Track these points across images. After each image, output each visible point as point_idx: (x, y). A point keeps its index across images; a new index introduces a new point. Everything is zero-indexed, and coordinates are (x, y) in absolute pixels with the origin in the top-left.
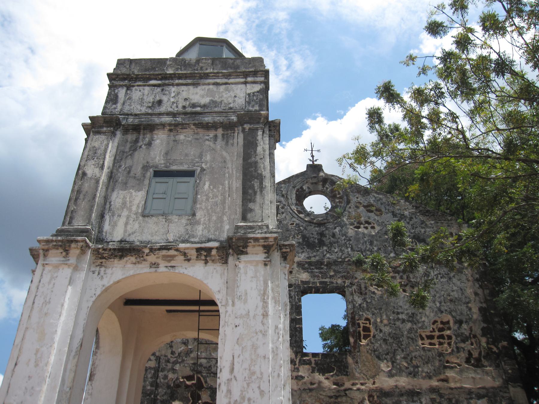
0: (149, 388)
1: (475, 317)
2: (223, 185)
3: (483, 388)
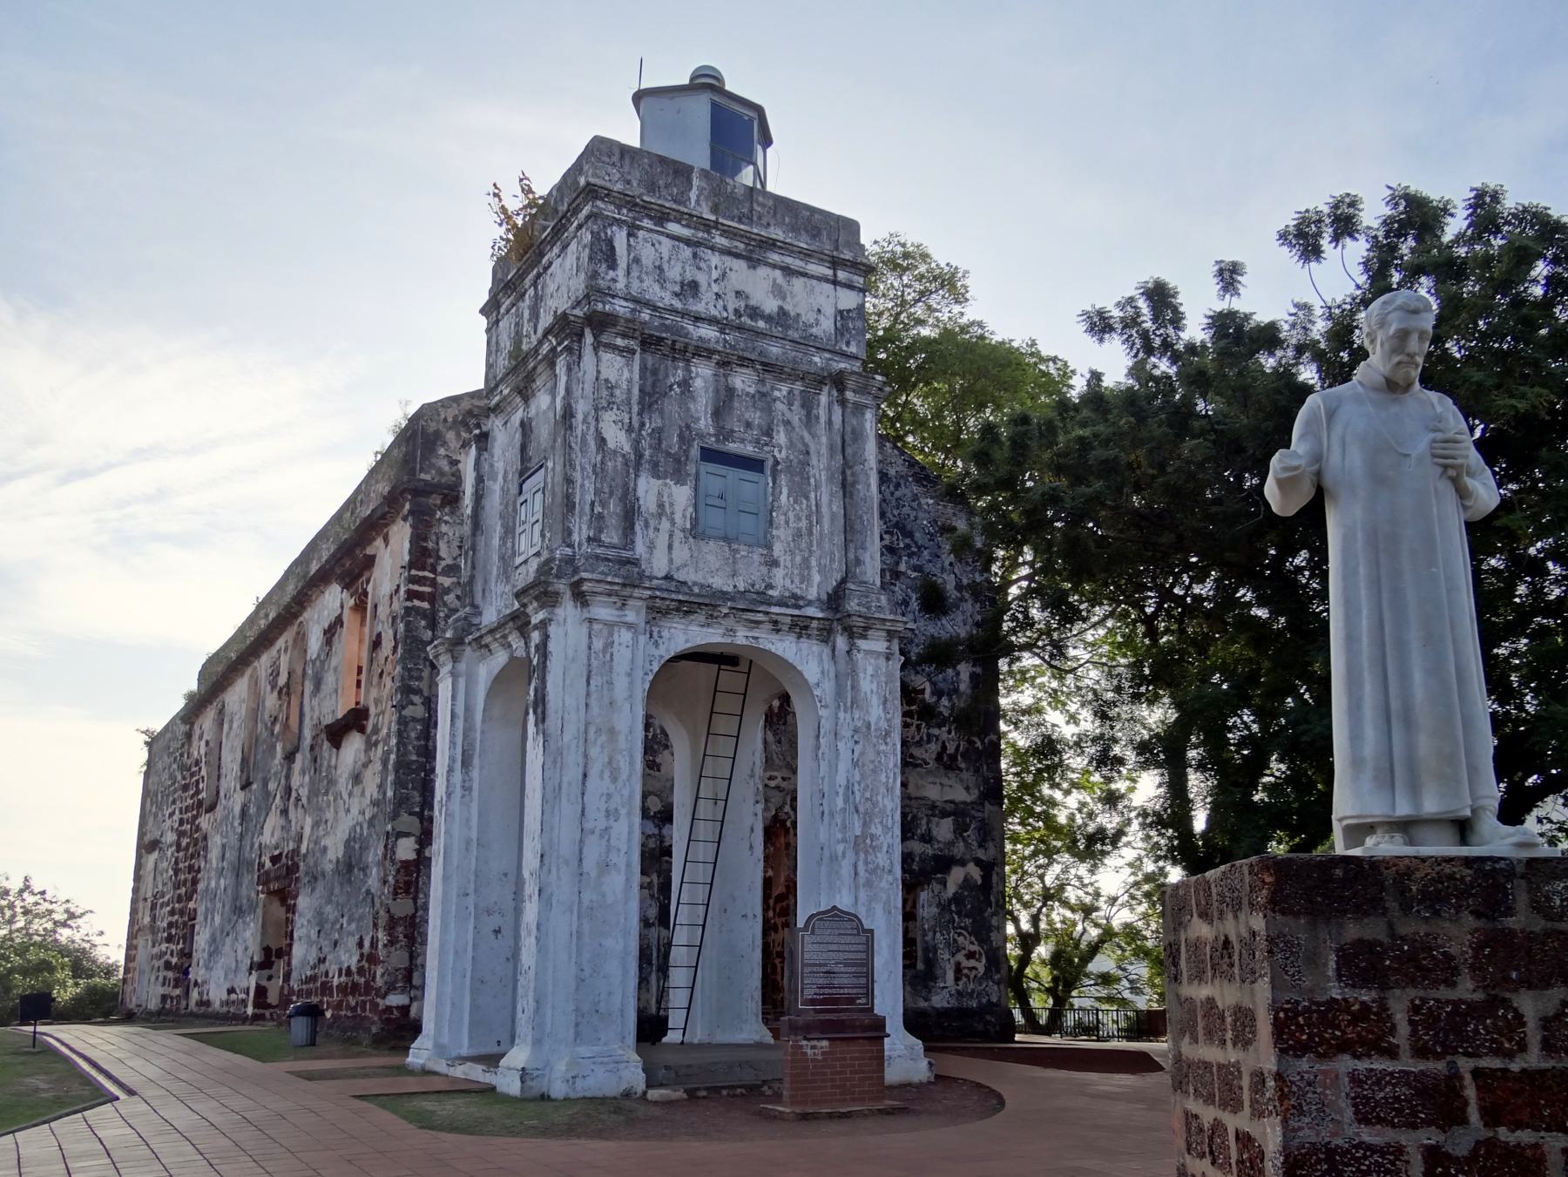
0: (414, 758)
1: (963, 687)
2: (807, 498)
3: (952, 802)
